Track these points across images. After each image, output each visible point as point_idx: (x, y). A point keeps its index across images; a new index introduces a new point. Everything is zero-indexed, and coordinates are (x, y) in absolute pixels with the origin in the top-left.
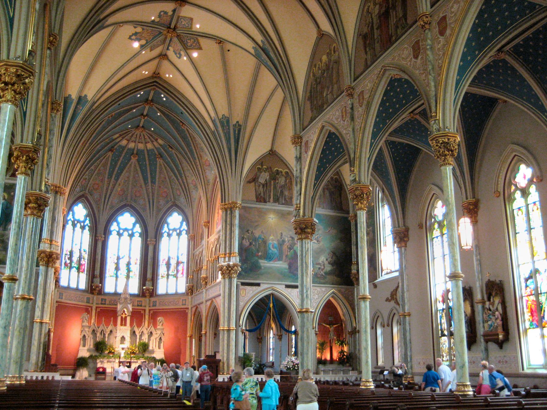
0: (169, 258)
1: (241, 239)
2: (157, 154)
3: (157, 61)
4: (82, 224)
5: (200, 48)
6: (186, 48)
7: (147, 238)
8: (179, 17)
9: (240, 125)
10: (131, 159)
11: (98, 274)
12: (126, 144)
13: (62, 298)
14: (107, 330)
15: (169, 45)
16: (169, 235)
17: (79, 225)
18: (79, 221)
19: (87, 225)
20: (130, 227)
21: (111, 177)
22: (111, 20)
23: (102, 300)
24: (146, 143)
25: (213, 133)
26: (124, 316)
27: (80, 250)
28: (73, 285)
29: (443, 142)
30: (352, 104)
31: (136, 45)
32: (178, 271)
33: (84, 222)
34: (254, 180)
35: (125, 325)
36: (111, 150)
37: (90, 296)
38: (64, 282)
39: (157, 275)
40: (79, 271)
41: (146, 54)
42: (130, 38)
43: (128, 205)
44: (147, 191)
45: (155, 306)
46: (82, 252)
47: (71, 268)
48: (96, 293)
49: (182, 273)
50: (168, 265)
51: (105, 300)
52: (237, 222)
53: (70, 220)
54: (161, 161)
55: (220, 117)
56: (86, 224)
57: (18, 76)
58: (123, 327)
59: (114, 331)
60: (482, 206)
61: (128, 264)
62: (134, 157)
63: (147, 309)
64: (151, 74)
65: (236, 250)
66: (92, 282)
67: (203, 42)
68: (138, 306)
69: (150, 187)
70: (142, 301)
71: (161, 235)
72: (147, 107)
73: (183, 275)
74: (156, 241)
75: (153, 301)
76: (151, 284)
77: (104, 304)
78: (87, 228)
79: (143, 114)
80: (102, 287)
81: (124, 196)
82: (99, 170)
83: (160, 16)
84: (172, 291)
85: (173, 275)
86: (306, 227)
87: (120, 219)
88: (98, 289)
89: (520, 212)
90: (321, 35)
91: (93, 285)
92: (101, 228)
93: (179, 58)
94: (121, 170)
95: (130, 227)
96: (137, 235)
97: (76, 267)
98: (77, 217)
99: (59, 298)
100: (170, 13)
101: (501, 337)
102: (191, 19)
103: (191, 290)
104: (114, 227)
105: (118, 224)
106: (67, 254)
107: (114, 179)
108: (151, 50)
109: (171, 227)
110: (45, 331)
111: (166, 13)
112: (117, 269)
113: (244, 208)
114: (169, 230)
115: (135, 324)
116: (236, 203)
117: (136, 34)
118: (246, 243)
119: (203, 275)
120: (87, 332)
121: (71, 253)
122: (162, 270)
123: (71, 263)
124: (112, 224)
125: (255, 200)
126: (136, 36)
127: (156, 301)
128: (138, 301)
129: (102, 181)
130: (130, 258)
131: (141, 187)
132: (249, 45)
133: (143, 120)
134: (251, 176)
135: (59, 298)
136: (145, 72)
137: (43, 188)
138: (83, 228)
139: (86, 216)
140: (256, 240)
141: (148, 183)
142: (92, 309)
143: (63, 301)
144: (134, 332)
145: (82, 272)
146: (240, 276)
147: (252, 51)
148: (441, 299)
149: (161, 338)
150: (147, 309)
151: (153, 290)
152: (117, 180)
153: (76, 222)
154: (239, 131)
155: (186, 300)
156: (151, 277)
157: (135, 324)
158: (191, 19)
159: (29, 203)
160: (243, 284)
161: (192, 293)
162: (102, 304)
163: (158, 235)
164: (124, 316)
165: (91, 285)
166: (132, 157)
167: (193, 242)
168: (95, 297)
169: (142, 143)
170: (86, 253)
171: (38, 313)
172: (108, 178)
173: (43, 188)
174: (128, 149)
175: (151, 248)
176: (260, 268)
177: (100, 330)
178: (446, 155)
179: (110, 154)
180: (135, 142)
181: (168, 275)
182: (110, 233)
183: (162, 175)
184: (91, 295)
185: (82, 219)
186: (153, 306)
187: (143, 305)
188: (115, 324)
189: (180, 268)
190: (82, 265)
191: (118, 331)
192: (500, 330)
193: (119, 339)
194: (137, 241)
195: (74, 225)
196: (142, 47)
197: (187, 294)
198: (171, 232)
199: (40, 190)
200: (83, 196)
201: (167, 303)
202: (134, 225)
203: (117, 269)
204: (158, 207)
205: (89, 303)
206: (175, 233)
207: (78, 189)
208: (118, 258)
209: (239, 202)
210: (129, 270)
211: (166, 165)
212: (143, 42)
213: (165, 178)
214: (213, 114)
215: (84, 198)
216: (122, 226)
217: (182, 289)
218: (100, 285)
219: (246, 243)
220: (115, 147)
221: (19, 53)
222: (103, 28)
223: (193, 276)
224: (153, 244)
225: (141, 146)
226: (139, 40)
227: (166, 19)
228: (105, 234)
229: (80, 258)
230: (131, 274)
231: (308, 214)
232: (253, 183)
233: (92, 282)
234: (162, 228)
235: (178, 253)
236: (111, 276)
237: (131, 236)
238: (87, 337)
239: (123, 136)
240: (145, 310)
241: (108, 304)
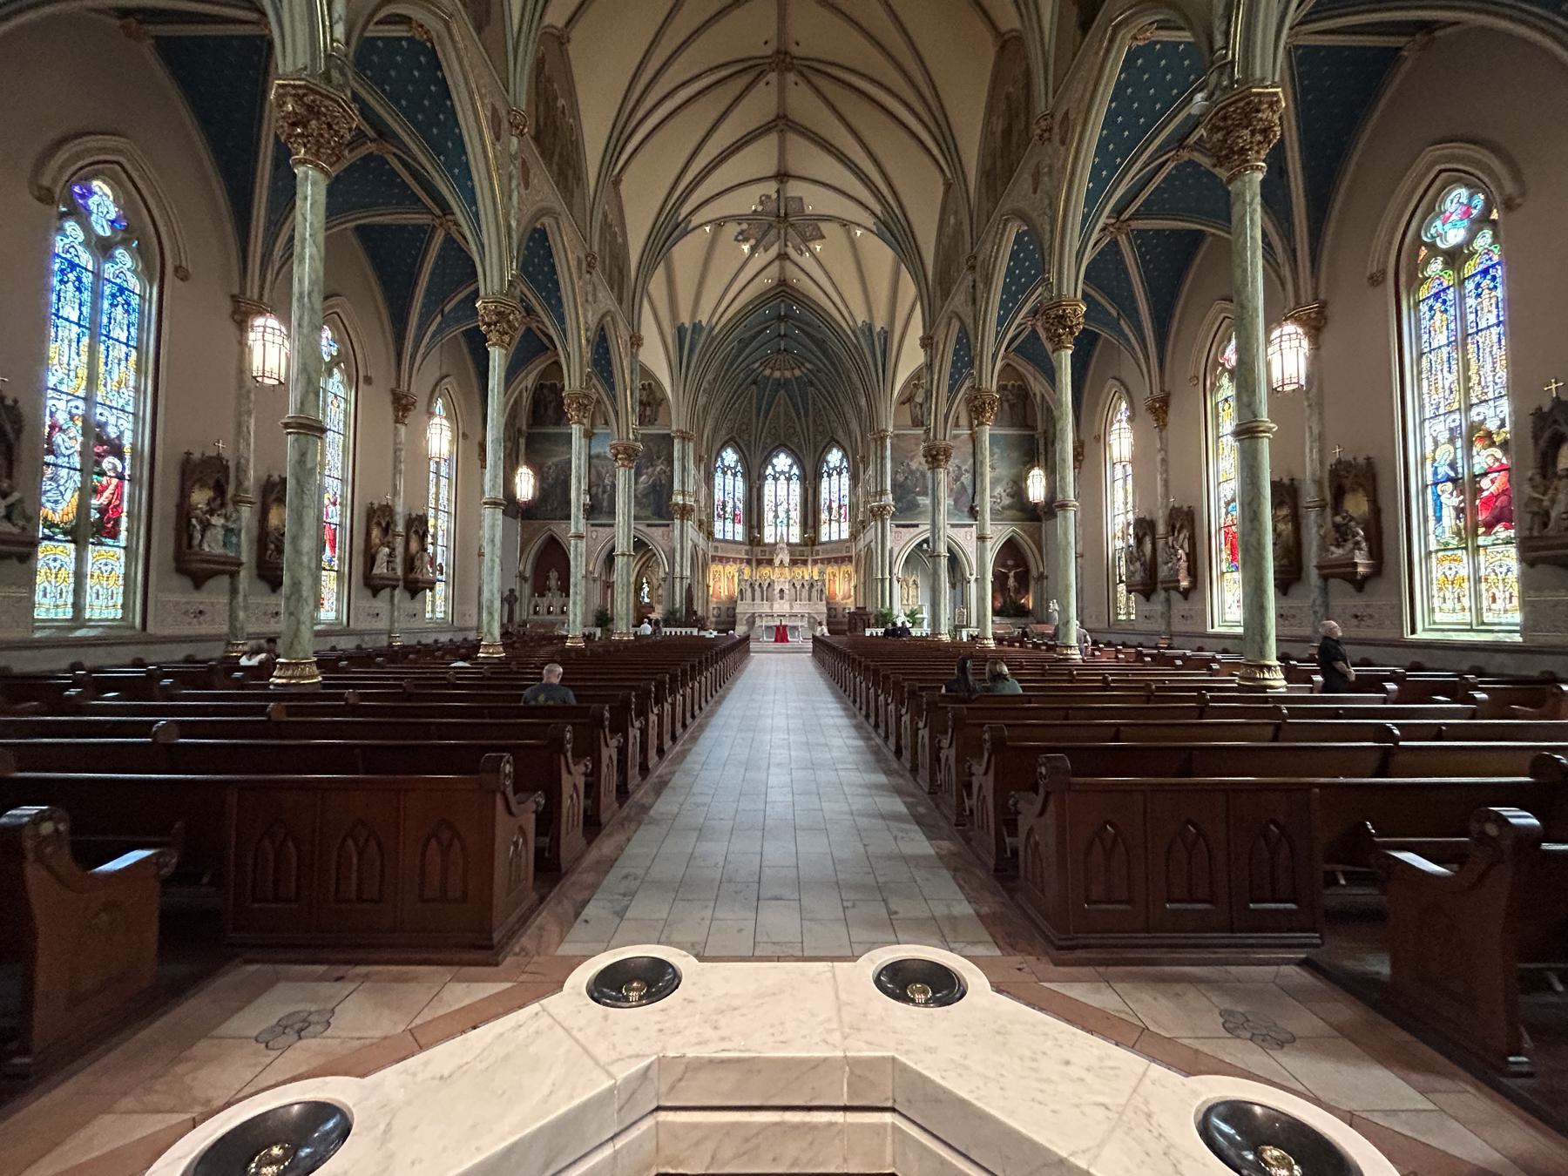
1: (895, 473)
3: (777, 263)
5: (823, 237)
6: (805, 240)
7: (805, 479)
8: (786, 198)
9: (886, 332)
10: (777, 391)
15: (786, 241)
16: (830, 476)
18: (729, 467)
20: (786, 469)
22: (696, 220)
25: (855, 347)
28: (729, 536)
29: (1057, 316)
30: (974, 281)
31: (746, 248)
32: (840, 515)
33: (735, 468)
34: (910, 399)
36: (755, 382)
38: (719, 535)
41: (761, 258)
42: (736, 239)
47: (725, 519)
50: (830, 509)
52: (888, 453)
55: (860, 323)
57: (499, 314)
60: (1174, 402)
61: (788, 511)
64: (776, 282)
65: (889, 488)
67: (825, 227)
72: (782, 326)
78: (739, 475)
83: (761, 203)
84: (835, 537)
86: (938, 454)
87: (775, 461)
89: (1227, 405)
90: (948, 186)
92: (755, 475)
93: (801, 254)
94: (770, 405)
95: (786, 469)
96: (795, 479)
98: (726, 464)
100: (774, 196)
101: (1184, 584)
102: (801, 199)
103: (854, 536)
104: (769, 470)
105: (774, 467)
108: (766, 250)
109: (832, 465)
110: (685, 585)
111: (768, 197)
112: (776, 517)
113: (896, 435)
116: (886, 431)
117: (741, 233)
118: (901, 478)
119: (860, 518)
121: (724, 502)
122: (824, 516)
125: (910, 423)
126: (743, 237)
132: (870, 222)
133: (782, 343)
134: (907, 394)
136: (766, 281)
137: (631, 436)
138: (735, 475)
139: (737, 462)
140: (912, 472)
146: (894, 517)
147: (874, 229)
148: (1120, 535)
154: (886, 339)
158: (801, 199)
159: (618, 453)
160: (897, 526)
163: (818, 477)
171: (678, 569)
173: (631, 436)
176: (918, 506)
178: (1060, 335)
179: (754, 387)
182: (765, 478)
185: (732, 465)
189: (842, 511)
192: (1183, 574)
194: (796, 486)
195: (725, 473)
196: (753, 249)
199: (628, 438)
200: (731, 439)
202: (791, 466)
203: (776, 517)
207: (723, 432)
208: (776, 506)
209: (891, 429)
212: (753, 242)
214: (851, 323)
216: (778, 469)
217: (845, 535)
219: (901, 478)
221: (496, 288)
222: (686, 233)
225: (788, 374)
226: (746, 240)
227: (772, 206)
229: (734, 507)
230: (791, 522)
231: (940, 436)
232: (907, 405)
237: (789, 479)
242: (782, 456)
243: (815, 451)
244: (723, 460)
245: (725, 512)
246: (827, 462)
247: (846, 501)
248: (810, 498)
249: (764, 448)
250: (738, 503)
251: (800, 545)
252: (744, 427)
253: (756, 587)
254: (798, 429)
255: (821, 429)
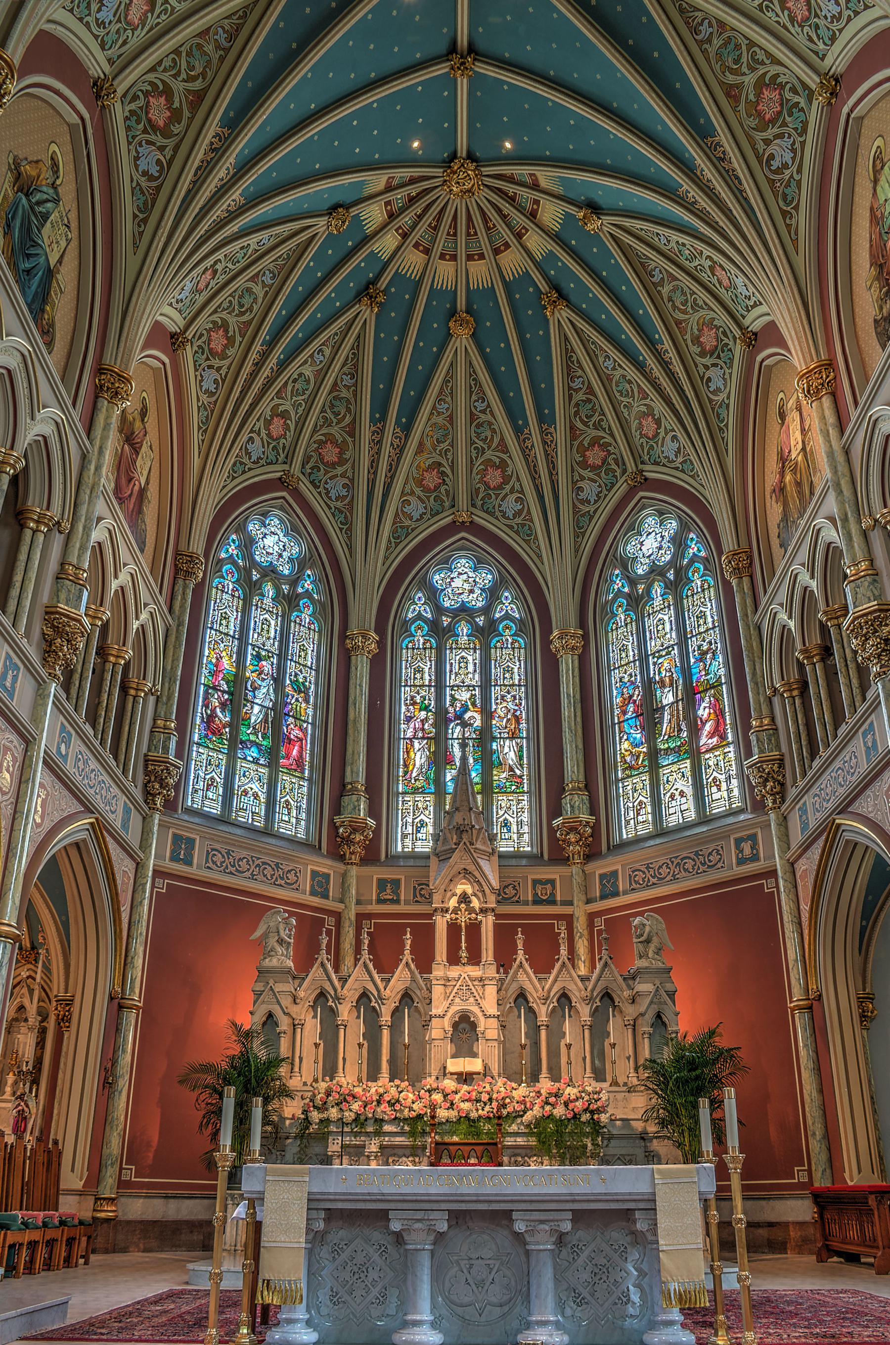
0: (649, 686)
2: (543, 286)
4: (285, 588)
10: (449, 335)
11: (362, 778)
12: (420, 267)
13: (189, 862)
14: (387, 993)
17: (269, 590)
18: (270, 572)
19: (308, 594)
20: (477, 600)
21: (383, 418)
23: (382, 884)
24: (497, 252)
26: (463, 919)
27: (278, 681)
32: (695, 729)
35: (475, 959)
37: (326, 866)
39: (608, 767)
40: (273, 764)
43: (463, 526)
44: (526, 457)
45: (616, 894)
46: (288, 690)
47: (235, 744)
48: (355, 859)
49: (718, 732)
51: (396, 883)
53: (231, 560)
54: (564, 314)
56: (300, 590)
58: (454, 972)
59: (418, 995)
62: (462, 323)
63: (580, 912)
66: (337, 809)
68: (537, 902)
69: (536, 438)
70: (552, 882)
71: (606, 612)
73: (723, 737)
74: (585, 637)
75: (602, 876)
76: (586, 807)
77: (397, 902)
79: (454, 42)
80: (377, 831)
81: (443, 489)
82: (335, 384)
85: (676, 750)
88: (358, 837)
91: (337, 820)
95: (477, 600)
97: (258, 746)
99: (174, 858)
105: (433, 595)
106: (215, 688)
107: (398, 423)
114: (632, 582)
115: (521, 956)
120: (286, 1001)
121: (238, 684)
123: (234, 726)
124: (407, 598)
127: (615, 873)
128: (535, 882)
129: (352, 431)
130: (487, 714)
131: (503, 447)
135: (174, 858)
141: (526, 424)
142: (338, 925)
143: (194, 871)
144: (522, 996)
145: (290, 771)
149: (659, 1016)
150: (580, 912)
151: (596, 828)
152: (407, 429)
153: (255, 576)
155: (753, 838)
156: (582, 777)
157: (521, 956)
161: (781, 793)
162: (380, 901)
164: (463, 919)
165: (332, 823)
166: (451, 324)
167: (746, 580)
168: (354, 871)
169: (482, 257)
170: (307, 701)
172: (372, 420)
174: (433, 293)
175: (568, 666)
177: (350, 992)
179: (366, 313)
180: (454, 258)
181: (654, 755)
183: (577, 384)
184: (329, 862)
186: (603, 897)
187: (558, 898)
188: (424, 963)
189: (703, 712)
190: (290, 740)
191: (438, 991)
193: (440, 1029)
197: (758, 806)
198: (641, 588)
200: (281, 483)
201: (664, 871)
202: (493, 594)
204: (576, 511)
205: (326, 897)
206: (657, 589)
208: (442, 719)
210: (488, 761)
211: (581, 324)
213: (591, 391)
215: (284, 494)
218: (371, 822)
220: (383, 283)
223: (773, 719)
224: (573, 649)
225: (480, 272)
228: (380, 629)
230: (500, 776)
233: (337, 809)
234: (605, 580)
235: (684, 655)
236: (416, 791)
238: (284, 1024)
239: (406, 219)
240: (569, 919)
241: (407, 903)
242: (463, 564)
243: (579, 533)
244: (248, 544)
245: (238, 720)
246: (625, 564)
247: (718, 668)
248: (568, 686)
249: (399, 534)
250: (294, 699)
251: (534, 859)
252: (330, 453)
253: (345, 1012)
254: (518, 464)
255: (594, 456)
